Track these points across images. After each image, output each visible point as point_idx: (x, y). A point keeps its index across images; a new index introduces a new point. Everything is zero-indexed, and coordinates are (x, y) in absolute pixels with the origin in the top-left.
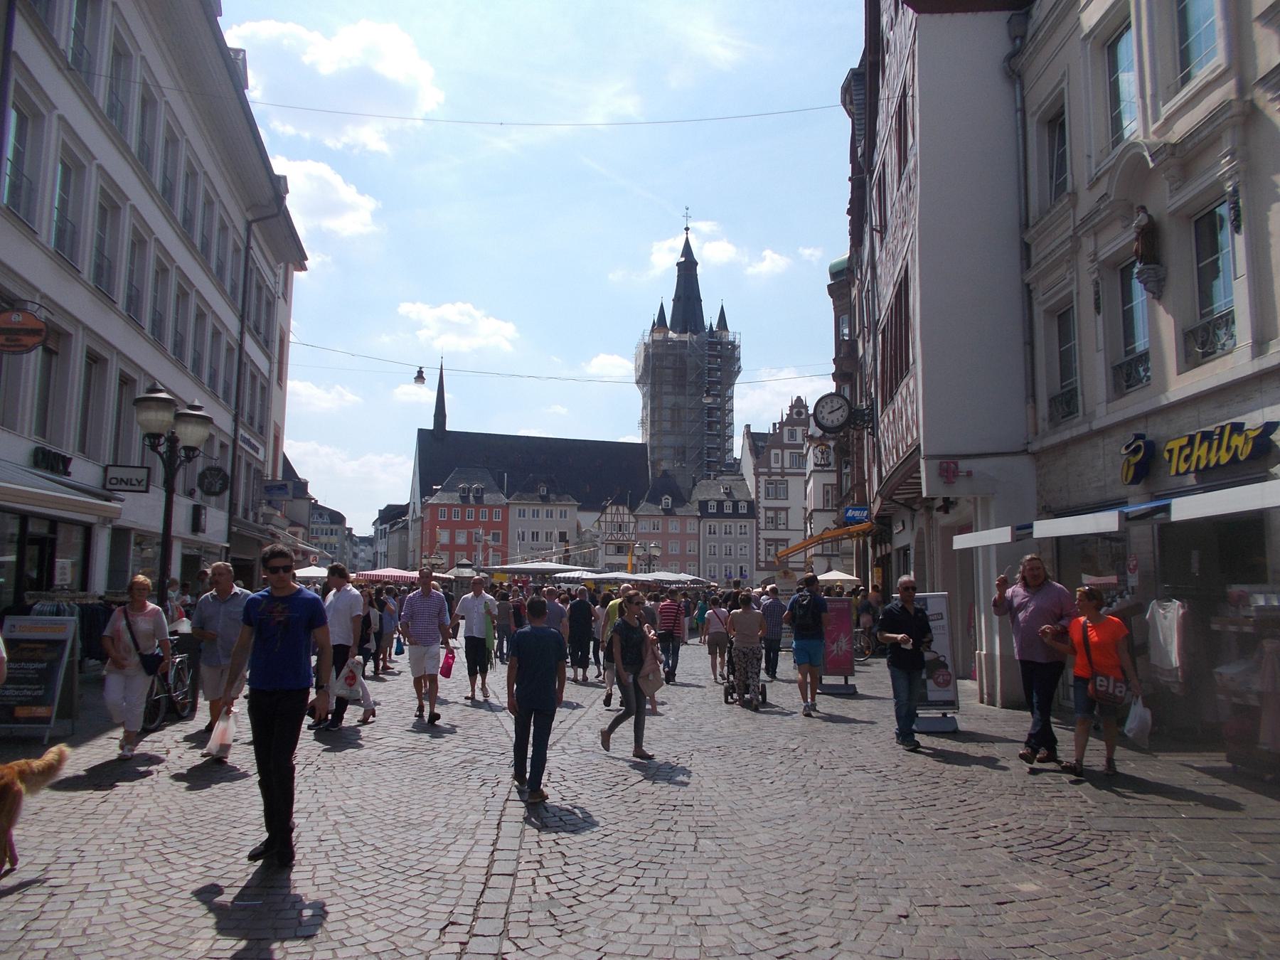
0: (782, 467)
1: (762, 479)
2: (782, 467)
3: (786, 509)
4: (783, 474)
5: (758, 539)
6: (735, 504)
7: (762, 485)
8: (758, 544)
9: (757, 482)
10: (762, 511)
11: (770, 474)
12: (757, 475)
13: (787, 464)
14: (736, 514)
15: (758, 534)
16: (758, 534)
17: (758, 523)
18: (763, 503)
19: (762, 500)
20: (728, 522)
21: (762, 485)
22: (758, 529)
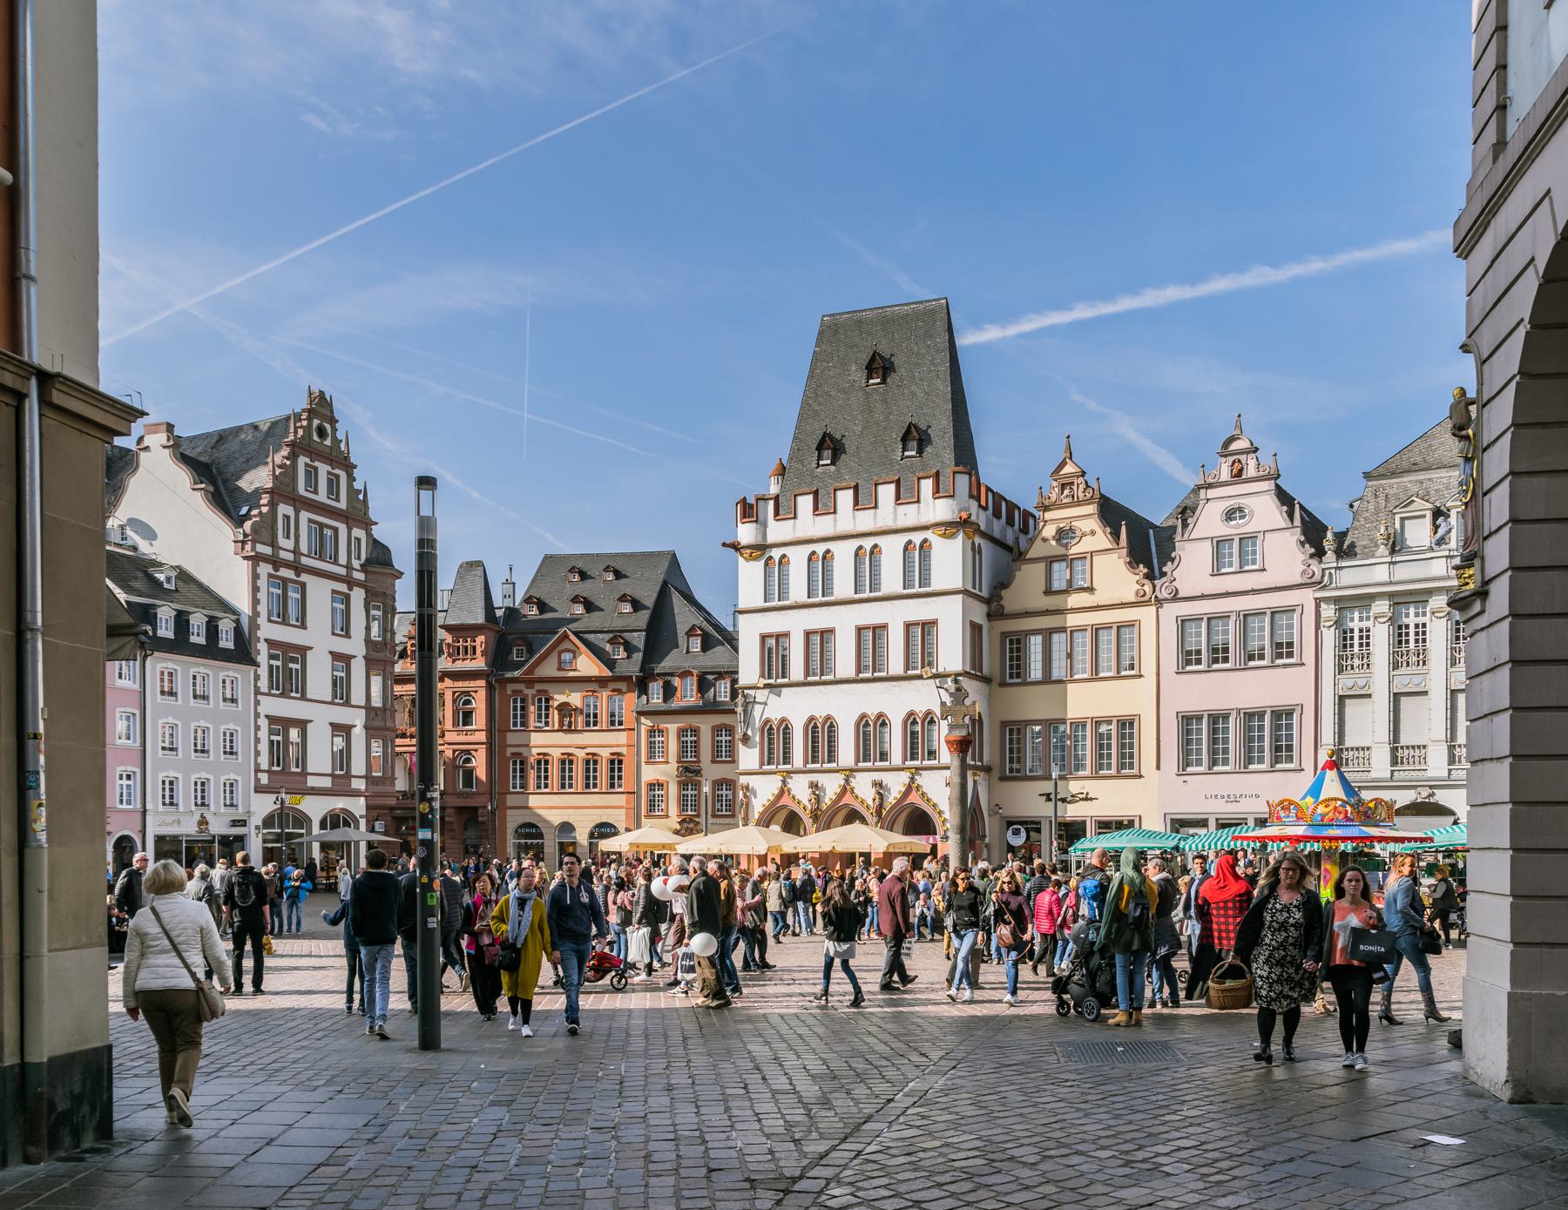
0: (296, 551)
1: (265, 569)
2: (296, 551)
3: (303, 650)
4: (298, 569)
5: (257, 715)
6: (182, 622)
7: (263, 583)
8: (257, 728)
9: (255, 576)
10: (262, 647)
11: (277, 563)
12: (256, 559)
13: (304, 548)
14: (211, 651)
15: (257, 703)
16: (257, 703)
17: (257, 677)
18: (268, 630)
19: (262, 620)
20: (201, 667)
21: (263, 583)
22: (257, 692)
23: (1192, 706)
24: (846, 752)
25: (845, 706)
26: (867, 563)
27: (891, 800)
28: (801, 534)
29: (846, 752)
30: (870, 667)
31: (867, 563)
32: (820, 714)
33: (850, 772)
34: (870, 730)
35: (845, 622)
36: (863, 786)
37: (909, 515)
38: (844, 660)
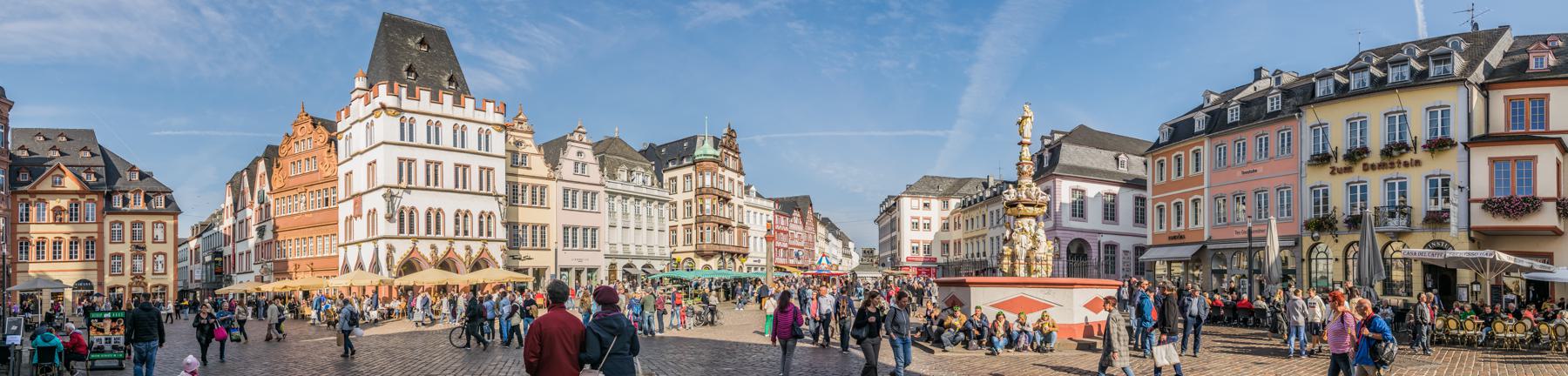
23: (568, 223)
24: (449, 230)
25: (450, 204)
26: (460, 135)
27: (474, 255)
28: (421, 109)
29: (449, 230)
30: (461, 187)
31: (460, 135)
32: (435, 206)
33: (452, 240)
34: (461, 216)
35: (449, 161)
36: (460, 248)
37: (480, 116)
38: (448, 182)
